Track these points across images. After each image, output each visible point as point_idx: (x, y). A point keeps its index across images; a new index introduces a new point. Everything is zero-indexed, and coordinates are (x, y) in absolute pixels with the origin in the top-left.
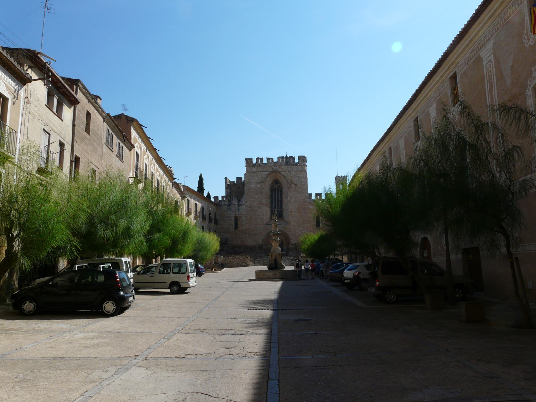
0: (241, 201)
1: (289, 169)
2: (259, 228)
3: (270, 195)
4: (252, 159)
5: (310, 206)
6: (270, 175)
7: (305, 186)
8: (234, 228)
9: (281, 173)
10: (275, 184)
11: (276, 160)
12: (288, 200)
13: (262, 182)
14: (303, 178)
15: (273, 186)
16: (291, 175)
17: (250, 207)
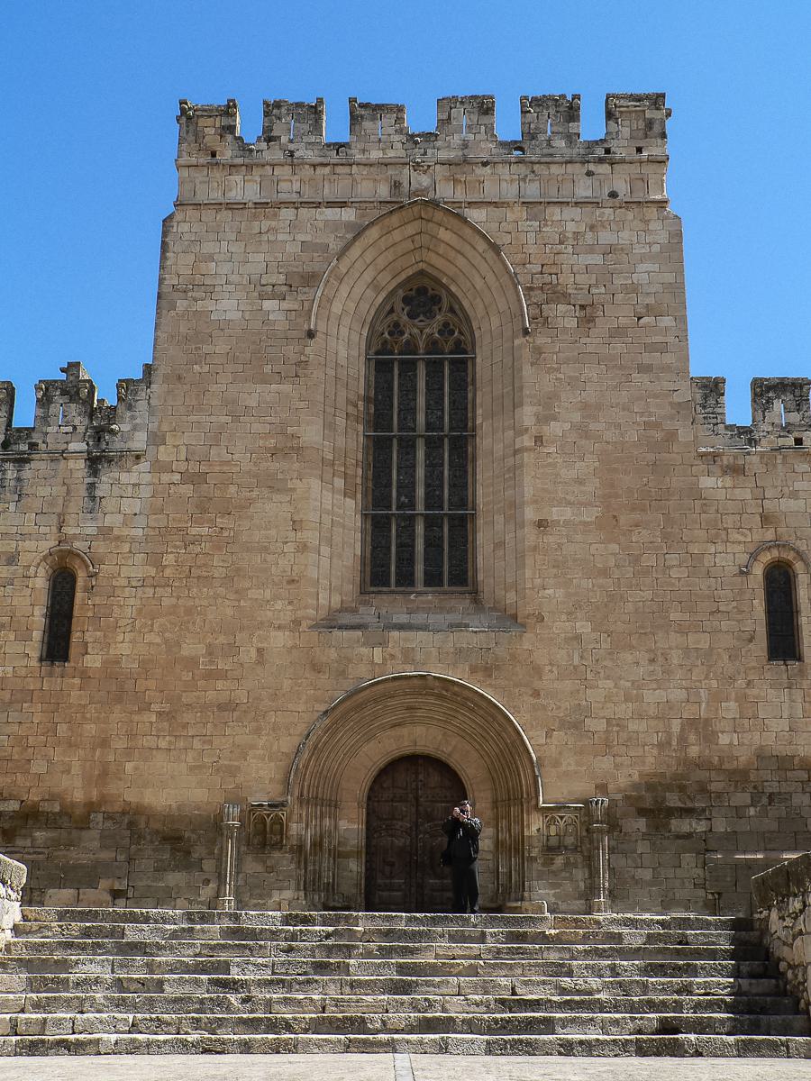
1: (532, 191)
2: (259, 651)
3: (367, 399)
4: (229, 110)
5: (707, 482)
6: (374, 233)
7: (667, 321)
8: (35, 654)
9: (465, 221)
10: (411, 316)
11: (421, 119)
13: (310, 279)
14: (643, 258)
15: (396, 329)
17: (187, 478)
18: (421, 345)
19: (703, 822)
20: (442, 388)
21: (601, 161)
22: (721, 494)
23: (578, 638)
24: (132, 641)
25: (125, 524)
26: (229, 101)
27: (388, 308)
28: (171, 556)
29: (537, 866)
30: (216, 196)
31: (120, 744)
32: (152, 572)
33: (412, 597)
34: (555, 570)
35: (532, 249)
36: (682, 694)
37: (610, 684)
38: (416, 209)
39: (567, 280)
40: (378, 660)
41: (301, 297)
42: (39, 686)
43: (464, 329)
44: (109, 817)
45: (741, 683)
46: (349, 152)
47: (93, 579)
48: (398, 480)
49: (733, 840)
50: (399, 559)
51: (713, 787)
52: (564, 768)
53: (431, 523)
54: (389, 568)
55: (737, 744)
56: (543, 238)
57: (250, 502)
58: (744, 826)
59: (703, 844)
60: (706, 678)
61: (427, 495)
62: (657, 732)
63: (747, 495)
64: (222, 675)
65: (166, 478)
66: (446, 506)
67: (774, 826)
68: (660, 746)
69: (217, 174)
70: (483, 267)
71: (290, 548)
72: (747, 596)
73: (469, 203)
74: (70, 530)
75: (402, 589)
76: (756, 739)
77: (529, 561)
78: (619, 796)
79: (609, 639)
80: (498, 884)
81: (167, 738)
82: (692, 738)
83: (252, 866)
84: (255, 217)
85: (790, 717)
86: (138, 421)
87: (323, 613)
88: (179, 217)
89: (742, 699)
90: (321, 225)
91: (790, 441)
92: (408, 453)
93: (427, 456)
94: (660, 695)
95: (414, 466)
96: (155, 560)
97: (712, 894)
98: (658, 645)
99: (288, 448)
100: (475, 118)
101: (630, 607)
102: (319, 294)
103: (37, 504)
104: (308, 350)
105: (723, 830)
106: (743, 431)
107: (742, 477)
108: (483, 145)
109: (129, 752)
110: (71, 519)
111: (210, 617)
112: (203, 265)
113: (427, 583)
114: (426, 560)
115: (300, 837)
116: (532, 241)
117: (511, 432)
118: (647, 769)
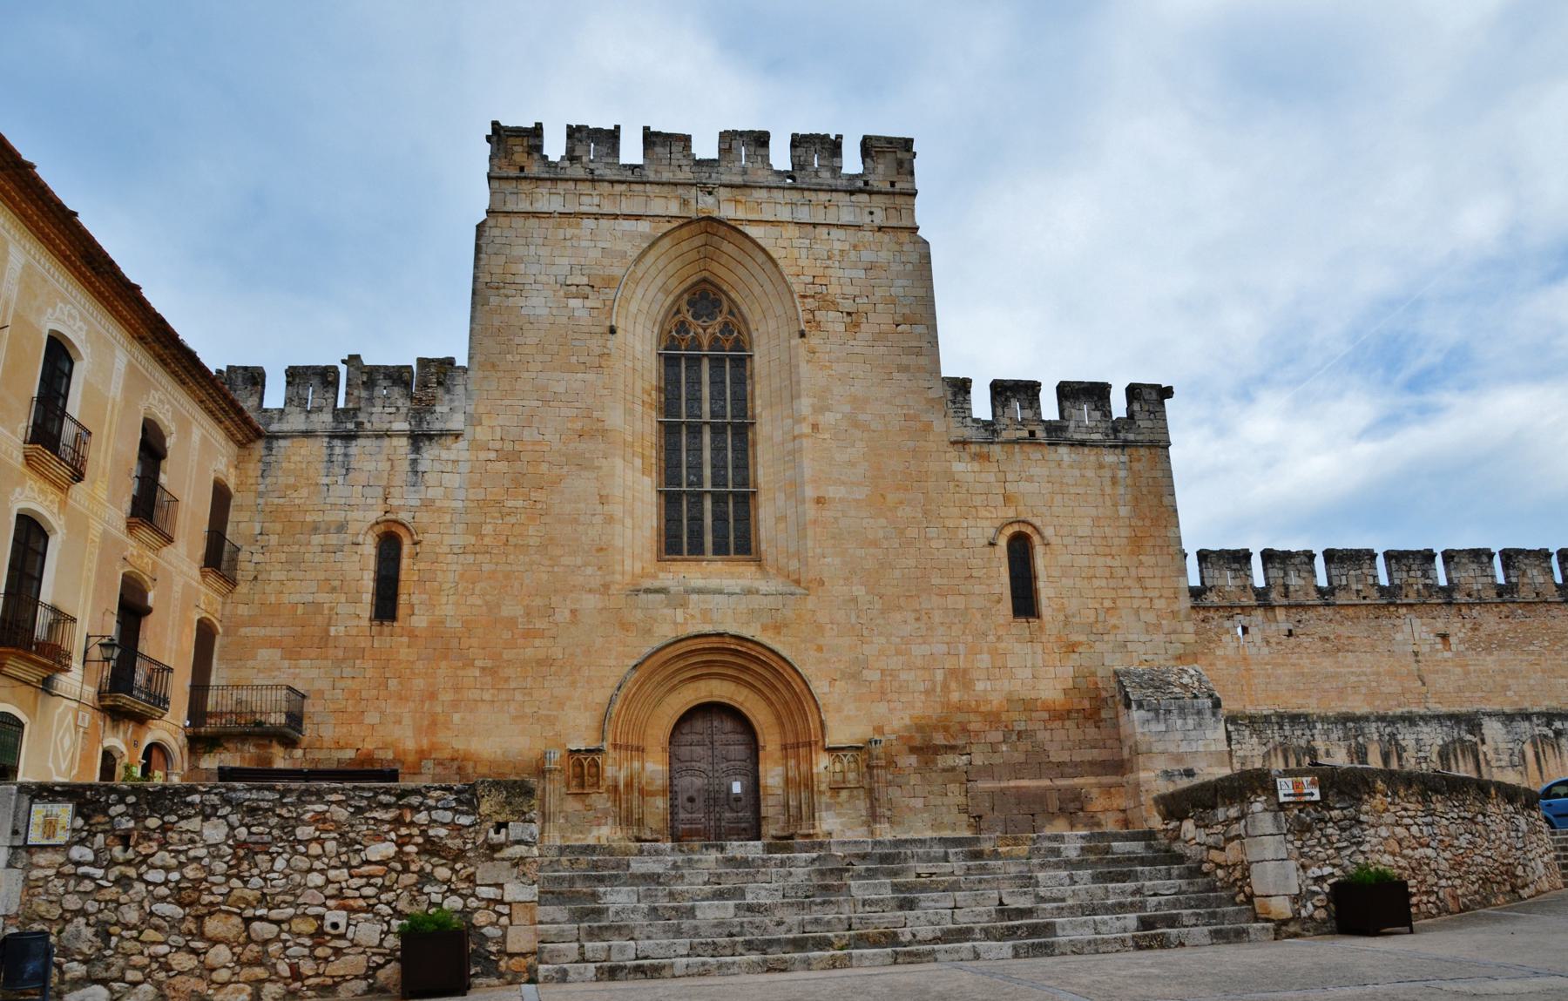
0: (438, 409)
1: (804, 214)
2: (573, 612)
3: (659, 389)
4: (537, 131)
6: (666, 242)
9: (746, 236)
10: (696, 316)
11: (705, 147)
12: (798, 420)
13: (609, 282)
15: (682, 327)
16: (821, 249)
18: (705, 343)
19: (964, 757)
20: (723, 382)
21: (861, 191)
22: (970, 477)
23: (855, 600)
24: (456, 604)
25: (446, 497)
26: (536, 124)
27: (675, 309)
28: (489, 526)
29: (825, 799)
30: (524, 206)
31: (446, 697)
32: (473, 540)
33: (704, 563)
34: (833, 542)
35: (803, 262)
36: (944, 648)
37: (883, 640)
38: (703, 223)
39: (834, 289)
40: (680, 619)
41: (602, 297)
42: (369, 644)
43: (743, 329)
44: (440, 763)
45: (992, 638)
46: (644, 173)
47: (418, 547)
48: (688, 461)
49: (989, 771)
50: (691, 531)
51: (972, 727)
52: (845, 713)
53: (719, 499)
54: (682, 539)
55: (990, 690)
56: (813, 254)
57: (561, 479)
58: (997, 760)
59: (968, 777)
60: (964, 633)
61: (714, 476)
62: (924, 681)
63: (993, 479)
64: (540, 634)
65: (483, 455)
66: (730, 484)
67: (1022, 758)
68: (927, 692)
69: (525, 186)
70: (762, 277)
71: (598, 520)
72: (994, 564)
73: (749, 221)
74: (394, 502)
75: (695, 557)
76: (1005, 686)
77: (810, 533)
78: (893, 737)
79: (881, 601)
80: (789, 816)
81: (491, 691)
82: (953, 685)
83: (572, 805)
84: (559, 226)
85: (1033, 666)
86: (456, 404)
87: (628, 578)
88: (491, 223)
89: (993, 652)
90: (619, 235)
91: (1027, 435)
92: (695, 438)
93: (713, 440)
94: (926, 649)
95: (701, 450)
96: (475, 529)
97: (974, 817)
98: (923, 606)
99: (594, 431)
100: (752, 149)
101: (897, 573)
102: (619, 295)
103: (362, 478)
104: (610, 344)
105: (981, 763)
106: (986, 425)
107: (987, 464)
108: (760, 172)
109: (455, 704)
110: (395, 492)
111: (527, 581)
112: (513, 266)
113: (716, 552)
114: (714, 531)
115: (616, 780)
116: (804, 255)
117: (790, 421)
118: (918, 712)
